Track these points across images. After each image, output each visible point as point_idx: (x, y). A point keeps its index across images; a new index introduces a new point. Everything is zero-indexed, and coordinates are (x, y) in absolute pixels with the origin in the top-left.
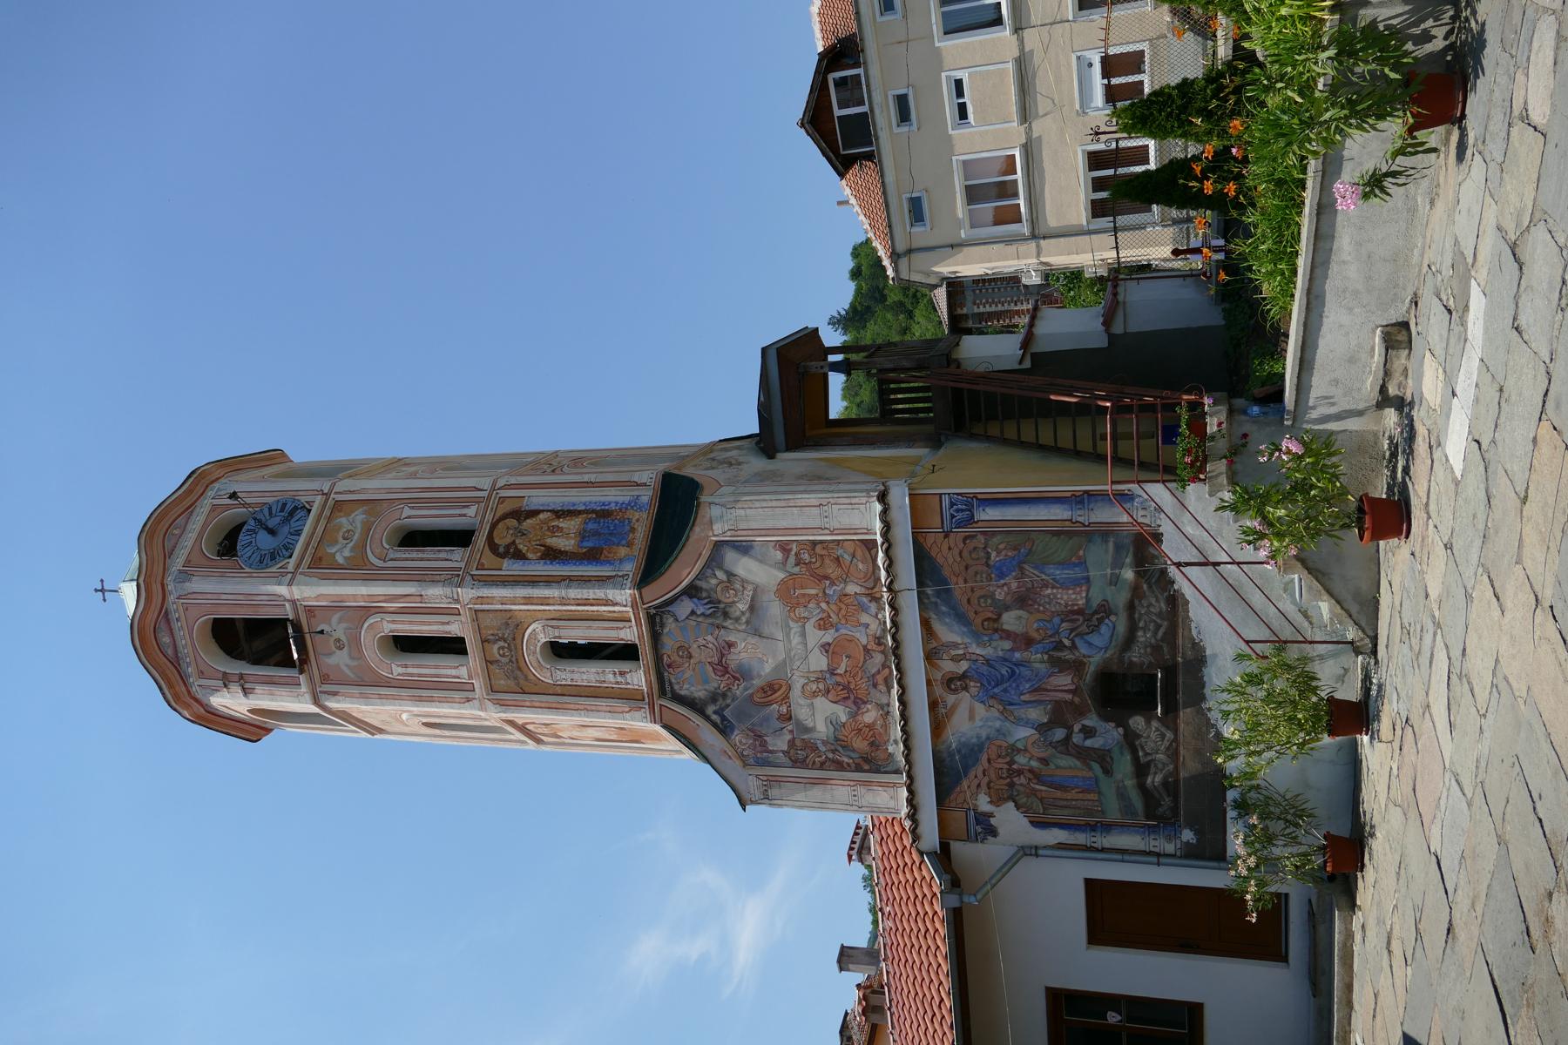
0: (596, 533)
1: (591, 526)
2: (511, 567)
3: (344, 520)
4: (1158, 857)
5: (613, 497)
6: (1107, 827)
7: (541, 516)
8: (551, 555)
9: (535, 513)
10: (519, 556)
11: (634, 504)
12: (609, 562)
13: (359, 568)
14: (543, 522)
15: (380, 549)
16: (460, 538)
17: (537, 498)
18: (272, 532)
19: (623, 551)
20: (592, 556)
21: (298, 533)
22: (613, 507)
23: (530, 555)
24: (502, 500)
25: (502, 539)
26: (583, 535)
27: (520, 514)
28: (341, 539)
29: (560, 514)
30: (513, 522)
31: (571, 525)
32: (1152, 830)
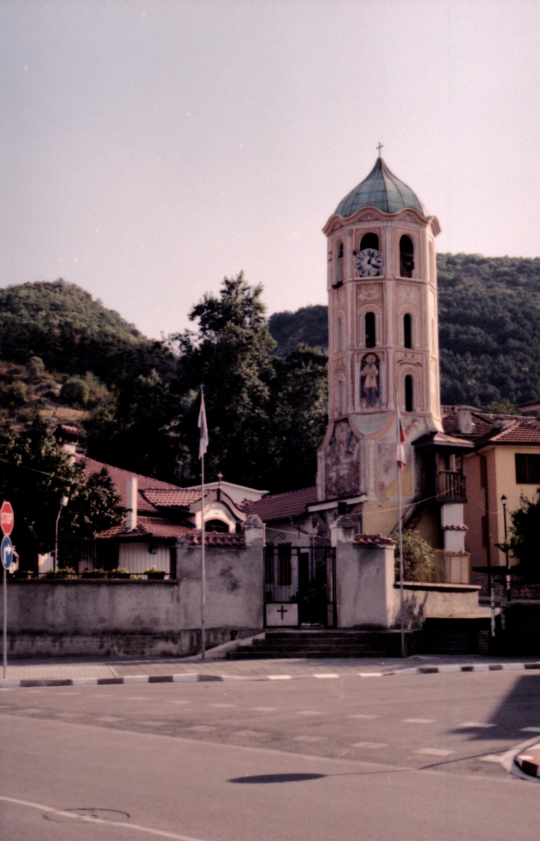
0: (371, 393)
1: (373, 391)
2: (358, 366)
3: (375, 290)
4: (312, 572)
5: (383, 396)
6: (316, 559)
7: (377, 371)
8: (363, 379)
9: (378, 367)
10: (362, 367)
11: (381, 404)
12: (361, 401)
13: (359, 303)
14: (374, 372)
15: (363, 311)
16: (371, 342)
17: (383, 367)
18: (369, 262)
19: (364, 405)
20: (363, 394)
21: (369, 274)
22: (380, 396)
23: (363, 372)
24: (383, 353)
25: (370, 359)
26: (370, 389)
27: (377, 363)
28: (367, 293)
29: (378, 378)
30: (374, 360)
31: (374, 384)
32: (316, 569)
